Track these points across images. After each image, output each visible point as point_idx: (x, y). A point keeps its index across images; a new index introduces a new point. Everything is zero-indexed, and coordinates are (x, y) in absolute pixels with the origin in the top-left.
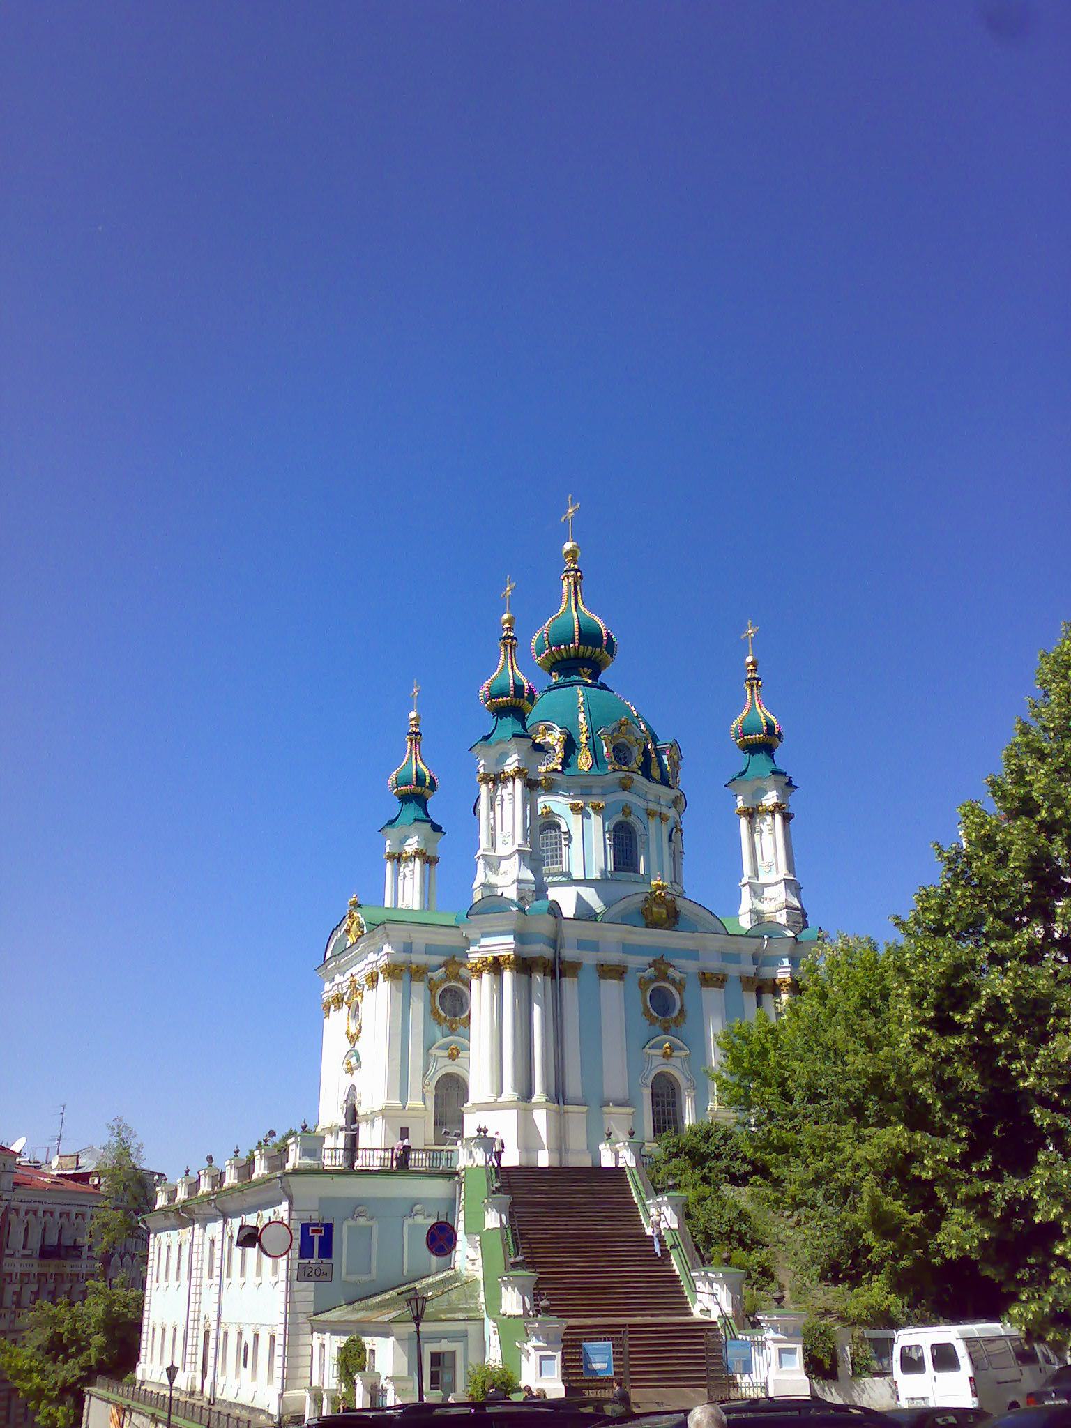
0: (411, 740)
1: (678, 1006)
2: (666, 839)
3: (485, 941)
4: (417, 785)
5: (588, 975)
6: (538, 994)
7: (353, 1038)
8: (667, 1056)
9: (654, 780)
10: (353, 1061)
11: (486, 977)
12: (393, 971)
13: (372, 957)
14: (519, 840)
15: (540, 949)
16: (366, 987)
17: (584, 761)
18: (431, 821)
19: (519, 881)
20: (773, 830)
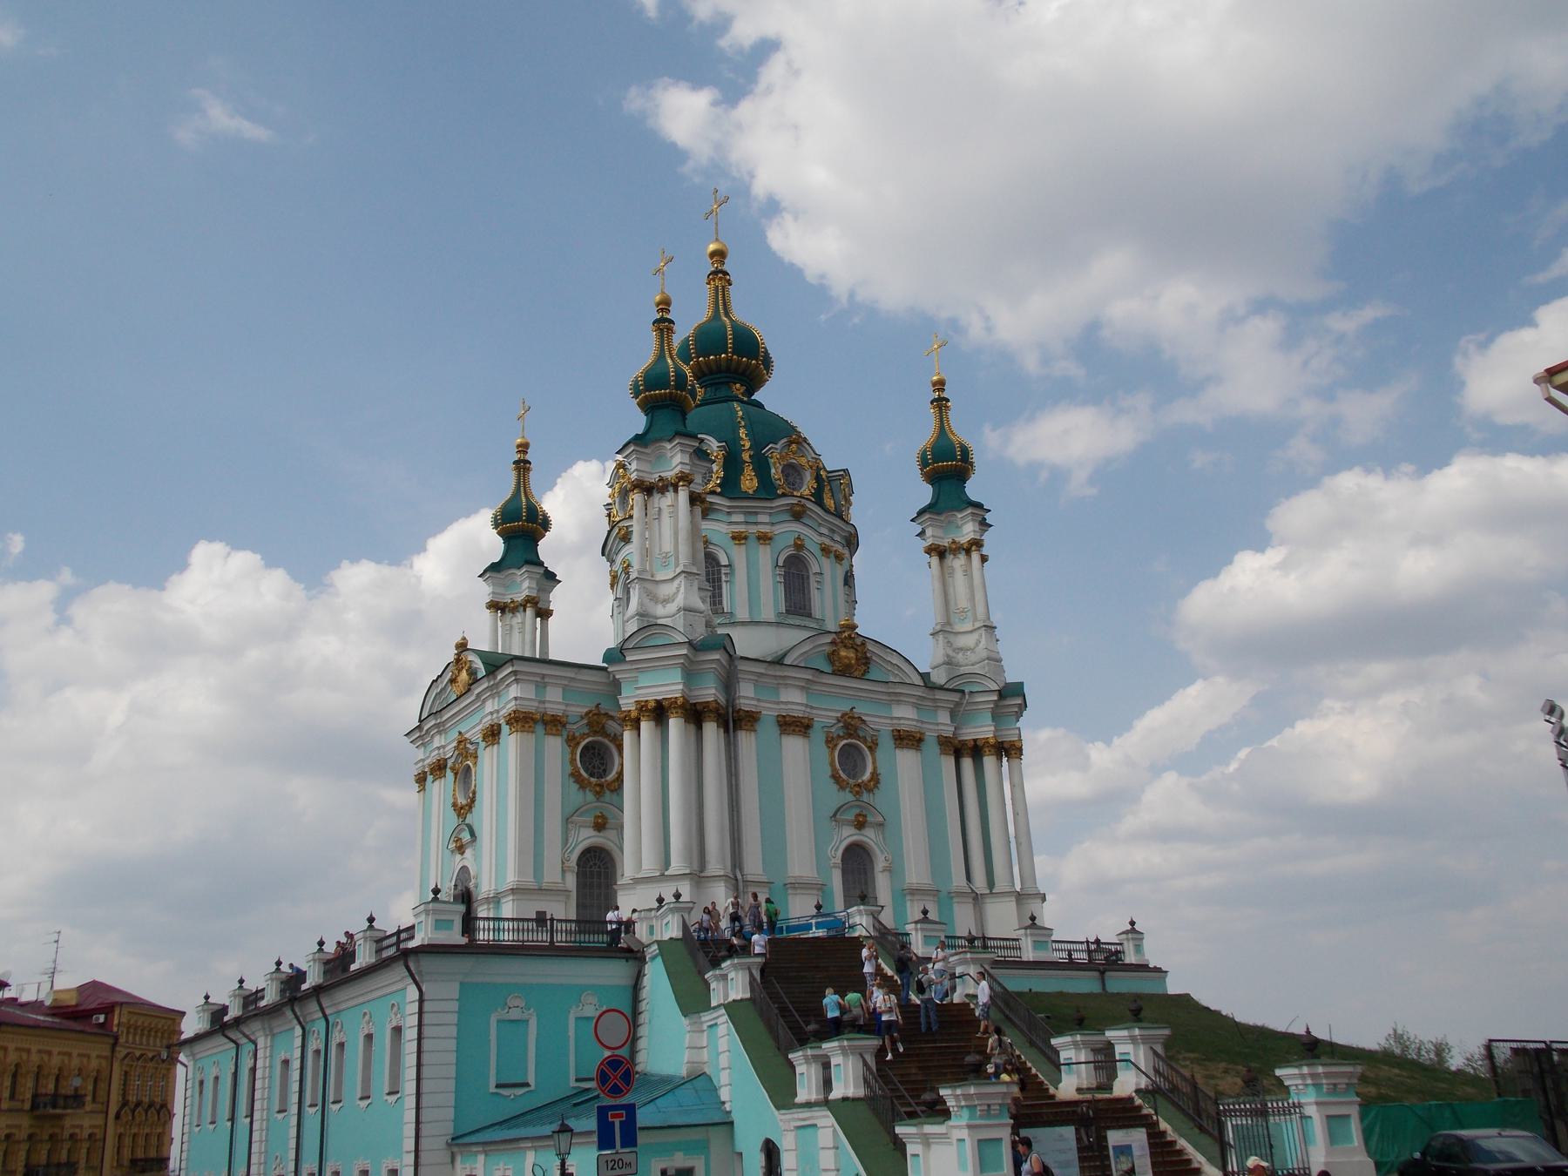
0: (518, 469)
1: (869, 769)
2: (840, 581)
3: (645, 680)
4: (528, 521)
5: (767, 728)
7: (463, 810)
8: (860, 824)
9: (827, 511)
10: (466, 836)
11: (646, 726)
12: (521, 720)
13: (490, 706)
14: (684, 560)
15: (709, 692)
16: (483, 744)
17: (749, 482)
18: (541, 564)
19: (687, 609)
20: (968, 573)
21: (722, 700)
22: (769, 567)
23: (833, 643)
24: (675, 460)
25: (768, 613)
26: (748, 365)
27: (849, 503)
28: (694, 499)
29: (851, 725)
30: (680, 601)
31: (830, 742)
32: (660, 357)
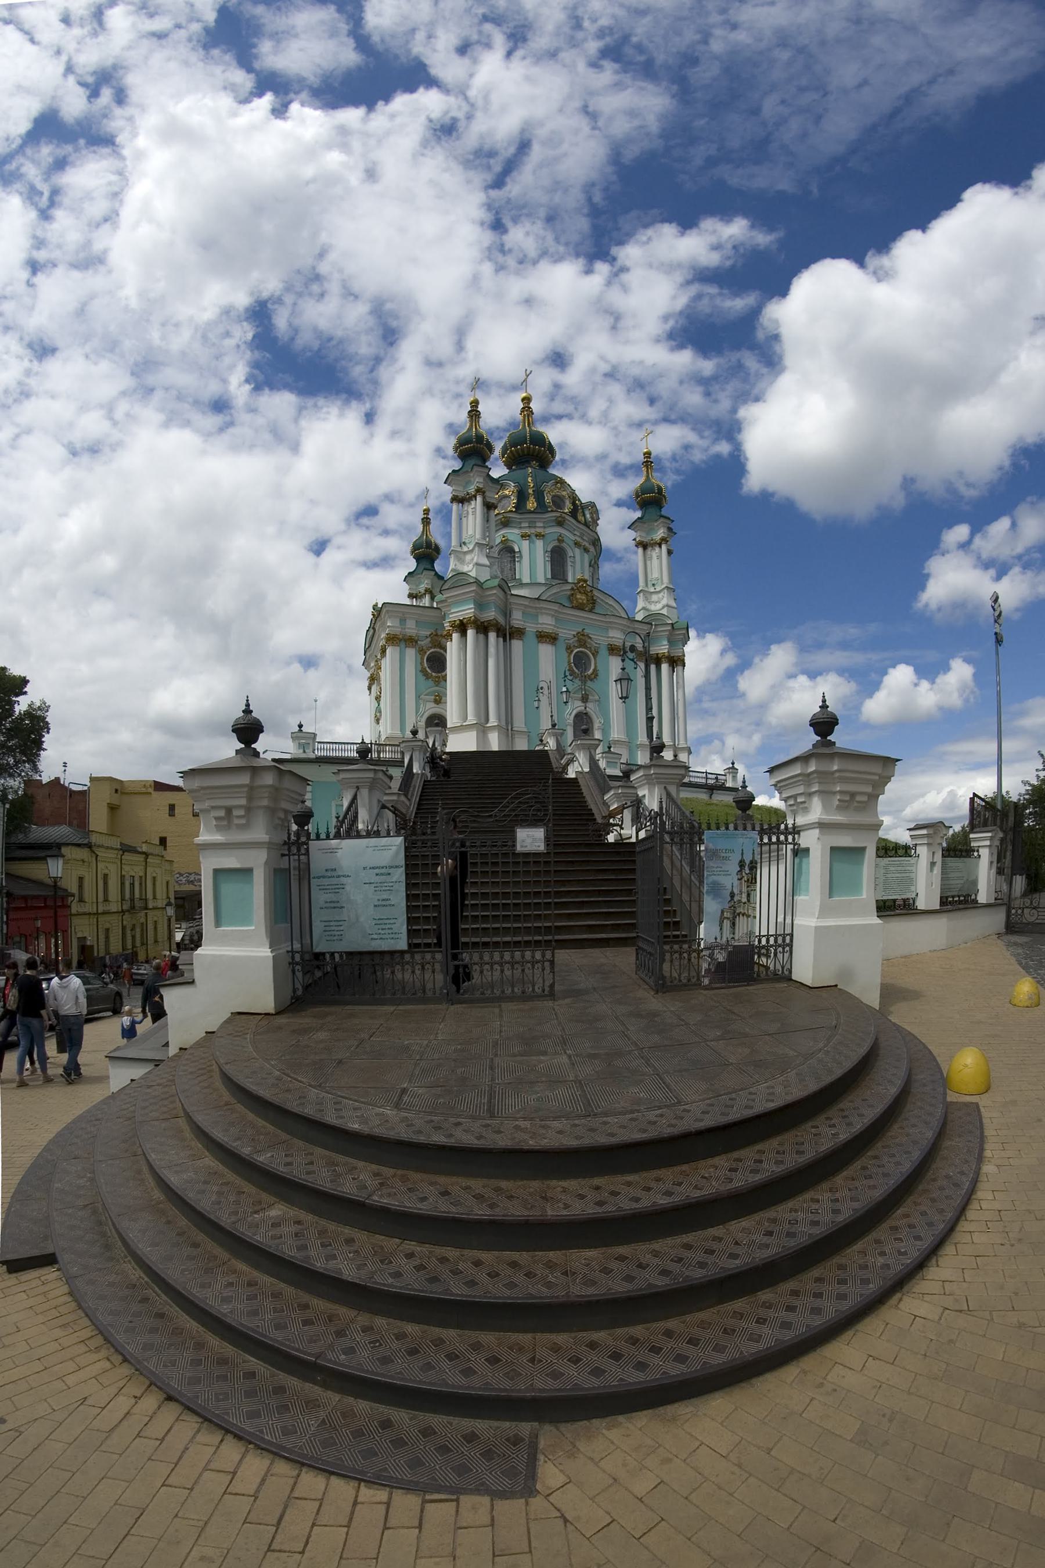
2: (587, 564)
6: (492, 650)
11: (455, 636)
14: (478, 536)
17: (531, 504)
19: (477, 564)
21: (501, 620)
22: (542, 552)
23: (572, 589)
24: (476, 481)
25: (541, 579)
26: (539, 450)
27: (595, 521)
28: (489, 506)
29: (582, 639)
30: (475, 561)
31: (569, 649)
32: (471, 426)
